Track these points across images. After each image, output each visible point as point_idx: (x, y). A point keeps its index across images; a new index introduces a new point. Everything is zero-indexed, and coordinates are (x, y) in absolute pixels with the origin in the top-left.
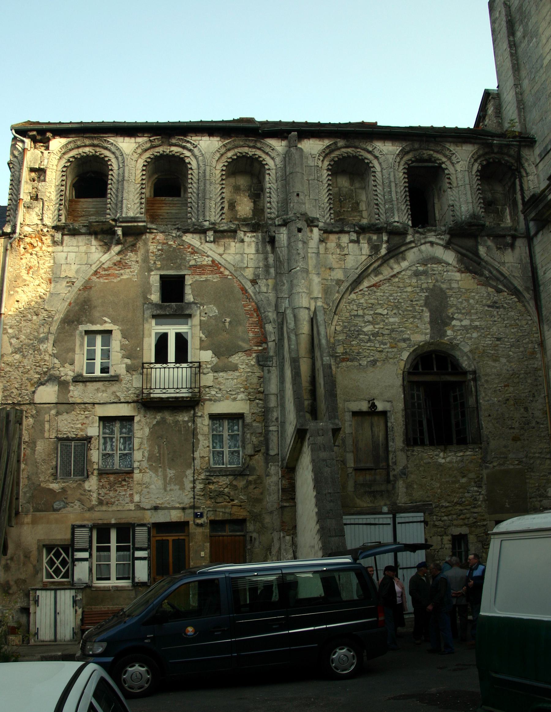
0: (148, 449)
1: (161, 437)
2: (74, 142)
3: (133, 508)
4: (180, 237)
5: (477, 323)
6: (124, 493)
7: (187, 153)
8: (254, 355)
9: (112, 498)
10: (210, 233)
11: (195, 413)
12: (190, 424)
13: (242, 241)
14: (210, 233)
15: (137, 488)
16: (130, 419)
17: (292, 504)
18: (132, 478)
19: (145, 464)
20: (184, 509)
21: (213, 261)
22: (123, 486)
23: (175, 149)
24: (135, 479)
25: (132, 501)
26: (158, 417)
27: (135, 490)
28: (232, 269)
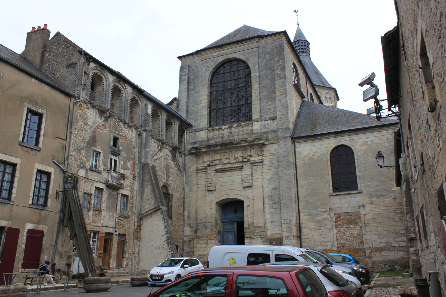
1: (110, 199)
2: (97, 67)
4: (119, 122)
7: (123, 90)
10: (127, 125)
13: (132, 131)
14: (127, 125)
15: (102, 218)
16: (102, 190)
20: (113, 228)
22: (99, 216)
23: (120, 86)
25: (101, 223)
26: (110, 190)
28: (130, 140)
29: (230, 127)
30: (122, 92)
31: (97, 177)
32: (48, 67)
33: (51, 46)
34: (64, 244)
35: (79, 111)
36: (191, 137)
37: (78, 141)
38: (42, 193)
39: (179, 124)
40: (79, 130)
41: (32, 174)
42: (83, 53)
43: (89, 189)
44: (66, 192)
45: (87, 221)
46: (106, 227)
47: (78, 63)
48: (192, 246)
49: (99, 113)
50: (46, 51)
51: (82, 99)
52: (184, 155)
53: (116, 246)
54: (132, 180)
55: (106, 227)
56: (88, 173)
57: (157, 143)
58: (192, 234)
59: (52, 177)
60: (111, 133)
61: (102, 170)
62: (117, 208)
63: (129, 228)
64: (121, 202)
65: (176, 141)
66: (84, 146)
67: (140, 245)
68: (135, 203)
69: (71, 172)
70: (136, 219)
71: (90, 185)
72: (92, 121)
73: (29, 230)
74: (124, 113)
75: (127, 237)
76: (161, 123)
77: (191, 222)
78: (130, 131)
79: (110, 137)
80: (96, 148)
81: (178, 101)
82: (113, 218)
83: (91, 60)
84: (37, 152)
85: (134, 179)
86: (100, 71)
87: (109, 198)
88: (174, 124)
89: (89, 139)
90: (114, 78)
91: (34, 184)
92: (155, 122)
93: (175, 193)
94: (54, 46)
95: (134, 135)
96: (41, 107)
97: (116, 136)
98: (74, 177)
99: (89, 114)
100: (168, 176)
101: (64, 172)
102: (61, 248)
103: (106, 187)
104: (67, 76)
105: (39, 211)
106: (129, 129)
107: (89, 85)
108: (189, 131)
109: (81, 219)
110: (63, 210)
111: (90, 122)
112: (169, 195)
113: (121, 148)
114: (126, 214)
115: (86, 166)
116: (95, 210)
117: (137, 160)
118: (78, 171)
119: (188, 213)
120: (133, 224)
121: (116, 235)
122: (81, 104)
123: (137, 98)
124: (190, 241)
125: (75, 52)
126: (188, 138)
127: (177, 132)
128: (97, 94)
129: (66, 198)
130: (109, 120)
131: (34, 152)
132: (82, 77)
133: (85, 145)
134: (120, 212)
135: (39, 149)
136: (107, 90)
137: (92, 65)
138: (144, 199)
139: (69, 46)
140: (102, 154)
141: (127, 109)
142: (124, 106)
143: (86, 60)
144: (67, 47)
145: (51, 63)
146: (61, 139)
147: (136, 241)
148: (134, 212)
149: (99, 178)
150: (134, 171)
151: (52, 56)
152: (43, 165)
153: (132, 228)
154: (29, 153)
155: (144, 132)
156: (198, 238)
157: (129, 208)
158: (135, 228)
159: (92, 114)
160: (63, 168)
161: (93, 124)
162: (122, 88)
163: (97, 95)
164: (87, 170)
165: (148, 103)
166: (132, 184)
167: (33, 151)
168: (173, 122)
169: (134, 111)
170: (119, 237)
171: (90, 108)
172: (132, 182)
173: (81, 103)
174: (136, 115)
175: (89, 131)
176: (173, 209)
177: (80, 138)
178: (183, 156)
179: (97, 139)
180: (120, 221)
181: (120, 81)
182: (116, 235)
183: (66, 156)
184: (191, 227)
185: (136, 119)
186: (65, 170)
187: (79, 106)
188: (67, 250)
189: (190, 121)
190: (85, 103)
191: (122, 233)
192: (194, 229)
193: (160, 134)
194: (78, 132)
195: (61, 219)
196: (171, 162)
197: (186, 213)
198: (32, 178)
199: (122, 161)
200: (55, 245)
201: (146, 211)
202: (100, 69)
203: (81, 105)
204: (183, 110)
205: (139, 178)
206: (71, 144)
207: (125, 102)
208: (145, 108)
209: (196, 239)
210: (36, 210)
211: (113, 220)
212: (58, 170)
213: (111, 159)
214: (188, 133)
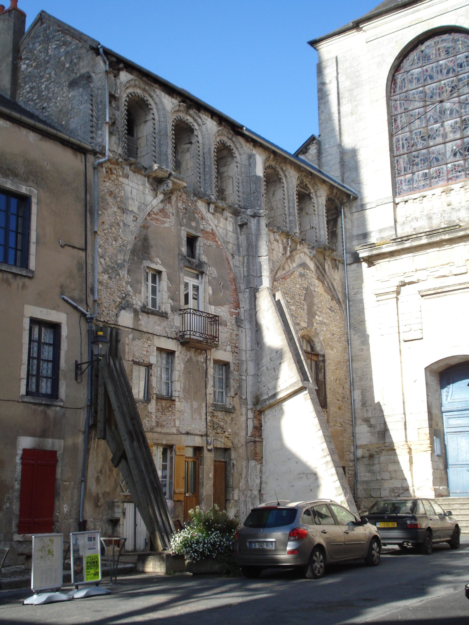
0: (183, 381)
3: (175, 432)
4: (196, 201)
5: (325, 321)
6: (170, 418)
7: (196, 127)
8: (234, 316)
9: (164, 421)
10: (212, 206)
11: (207, 357)
12: (204, 365)
13: (226, 219)
14: (212, 206)
15: (177, 413)
17: (261, 440)
18: (175, 405)
19: (181, 395)
20: (202, 436)
21: (212, 230)
24: (176, 407)
27: (176, 416)
29: (448, 191)
30: (196, 133)
31: (159, 325)
32: (28, 92)
33: (31, 46)
34: (102, 478)
35: (107, 184)
36: (356, 223)
37: (111, 251)
38: (47, 369)
39: (328, 195)
40: (111, 226)
41: (21, 329)
42: (101, 50)
43: (145, 353)
44: (95, 363)
45: (146, 423)
46: (188, 433)
47: (93, 75)
48: (376, 468)
49: (151, 184)
50: (21, 58)
51: (111, 155)
52: (343, 263)
53: (211, 475)
54: (235, 328)
55: (188, 433)
56: (139, 320)
57: (282, 241)
58: (374, 440)
59: (64, 332)
60: (181, 226)
61: (169, 311)
62: (208, 392)
63: (236, 434)
64: (214, 377)
65: (323, 234)
66: (124, 260)
67: (264, 471)
68: (244, 378)
69: (102, 320)
70: (250, 415)
71: (146, 345)
72: (136, 203)
73: (24, 450)
74: (205, 180)
75: (233, 455)
76: (286, 197)
77: (370, 415)
78: (222, 219)
79: (179, 236)
80: (152, 262)
81: (319, 144)
82: (200, 414)
83: (121, 65)
84: (26, 280)
85: (239, 326)
86: (144, 90)
87: (188, 372)
88: (317, 196)
89: (135, 244)
90: (176, 101)
91: (27, 351)
92: (273, 195)
93: (330, 351)
94: (37, 45)
95: (230, 228)
96: (26, 181)
97: (193, 232)
98: (109, 330)
99: (128, 189)
100: (311, 314)
101: (89, 320)
102: (94, 485)
103: (180, 347)
104: (73, 108)
105: (42, 408)
106: (218, 215)
107: (122, 122)
108: (351, 208)
109: (132, 419)
110: (91, 403)
111: (133, 206)
112: (317, 355)
113: (204, 258)
114: (228, 402)
115: (133, 305)
116: (161, 399)
117: (242, 282)
118: (117, 315)
119: (362, 393)
120: (244, 425)
121: (209, 450)
122: (110, 166)
123: (229, 143)
124: (371, 456)
125: (83, 51)
126: (349, 226)
127: (325, 214)
128: (142, 143)
129: (97, 376)
130: (174, 198)
131: (20, 281)
132: (105, 105)
133: (127, 257)
134: (215, 401)
135: (31, 275)
136: (163, 132)
137: (124, 76)
138: (265, 368)
139: (69, 39)
140: (164, 275)
141: (210, 167)
142: (202, 163)
143: (111, 65)
144: (65, 43)
145: (34, 84)
146: (74, 247)
147: (253, 463)
148: (244, 397)
149: (165, 328)
150: (237, 306)
151: (36, 67)
152: (41, 309)
153: (243, 433)
154: (9, 284)
155: (252, 219)
156: (388, 450)
157: (232, 390)
158: (249, 434)
159: (137, 187)
160: (84, 311)
161: (139, 209)
162: (195, 124)
163: (142, 145)
164: (136, 312)
165: (254, 152)
166: (234, 337)
167: (18, 278)
168: (312, 191)
169: (225, 174)
170: (215, 457)
171: (130, 173)
172: (235, 332)
173: (108, 165)
174: (231, 183)
175: (134, 227)
176: (328, 387)
177: (114, 243)
178: (340, 266)
179: (152, 242)
180: (215, 420)
181: (189, 108)
182: (209, 450)
183: (89, 285)
184: (370, 426)
185: (231, 191)
186: (88, 316)
187: (107, 172)
188: (108, 490)
189: (350, 186)
190: (118, 165)
191: (223, 446)
192: (378, 429)
193: (288, 221)
194: (110, 230)
195: (91, 422)
196: (316, 282)
197: (357, 395)
198: (20, 337)
199: (210, 288)
200: (82, 481)
201: (270, 395)
202: (142, 85)
203: (111, 169)
204: (332, 163)
205: (250, 322)
206: (97, 258)
207: (204, 154)
208: (250, 165)
209: (384, 452)
210: (37, 406)
211: (201, 419)
212: (76, 315)
213: (186, 285)
214: (348, 214)
